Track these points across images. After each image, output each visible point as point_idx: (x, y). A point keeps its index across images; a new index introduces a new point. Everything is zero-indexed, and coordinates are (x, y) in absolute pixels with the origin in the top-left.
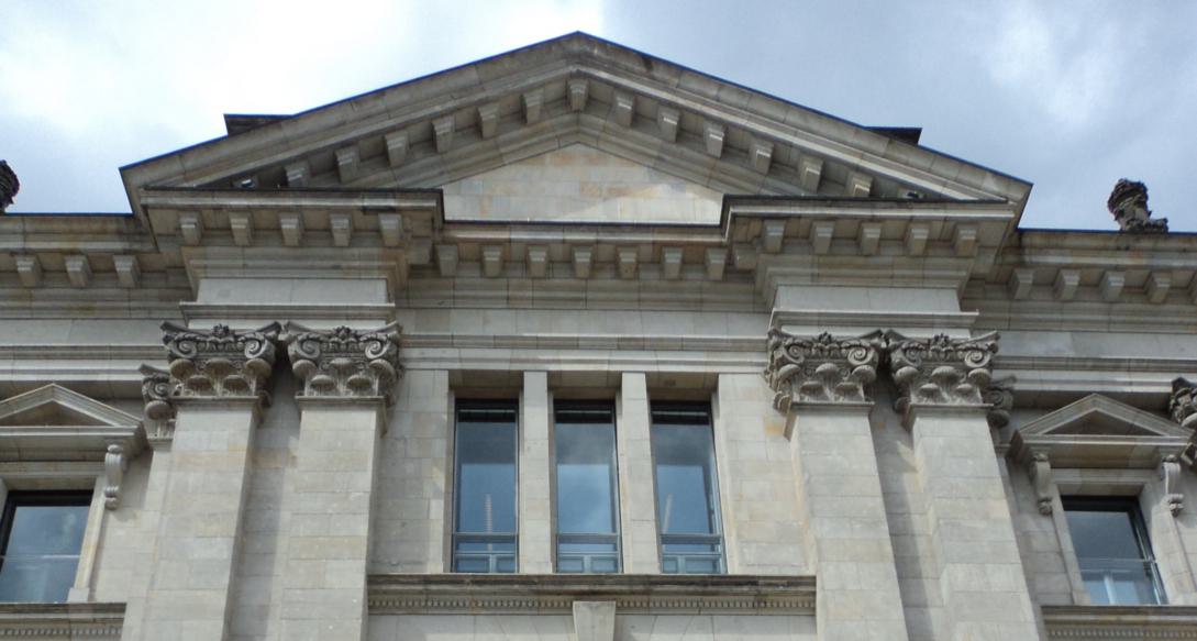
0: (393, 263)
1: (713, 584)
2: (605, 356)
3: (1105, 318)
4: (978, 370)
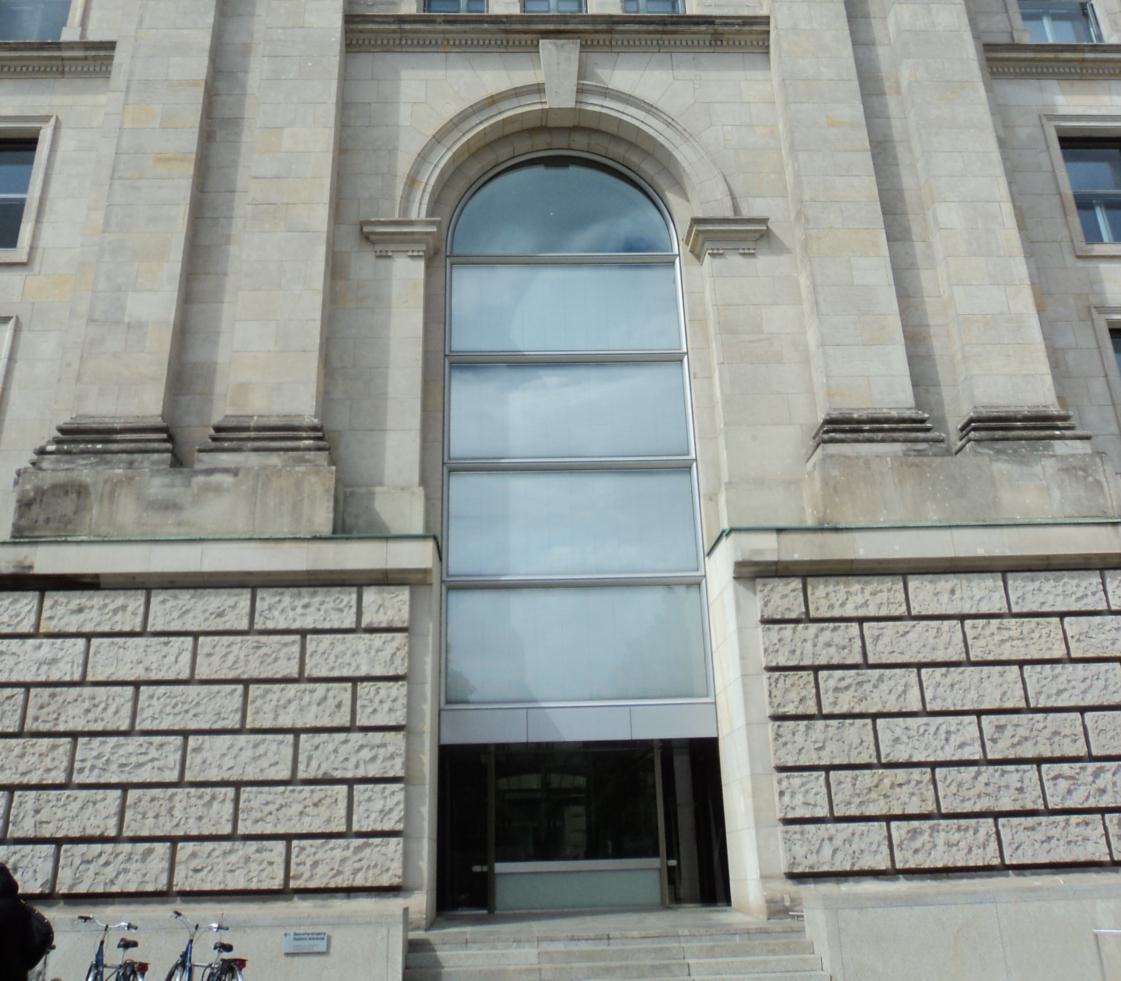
1: (673, 23)
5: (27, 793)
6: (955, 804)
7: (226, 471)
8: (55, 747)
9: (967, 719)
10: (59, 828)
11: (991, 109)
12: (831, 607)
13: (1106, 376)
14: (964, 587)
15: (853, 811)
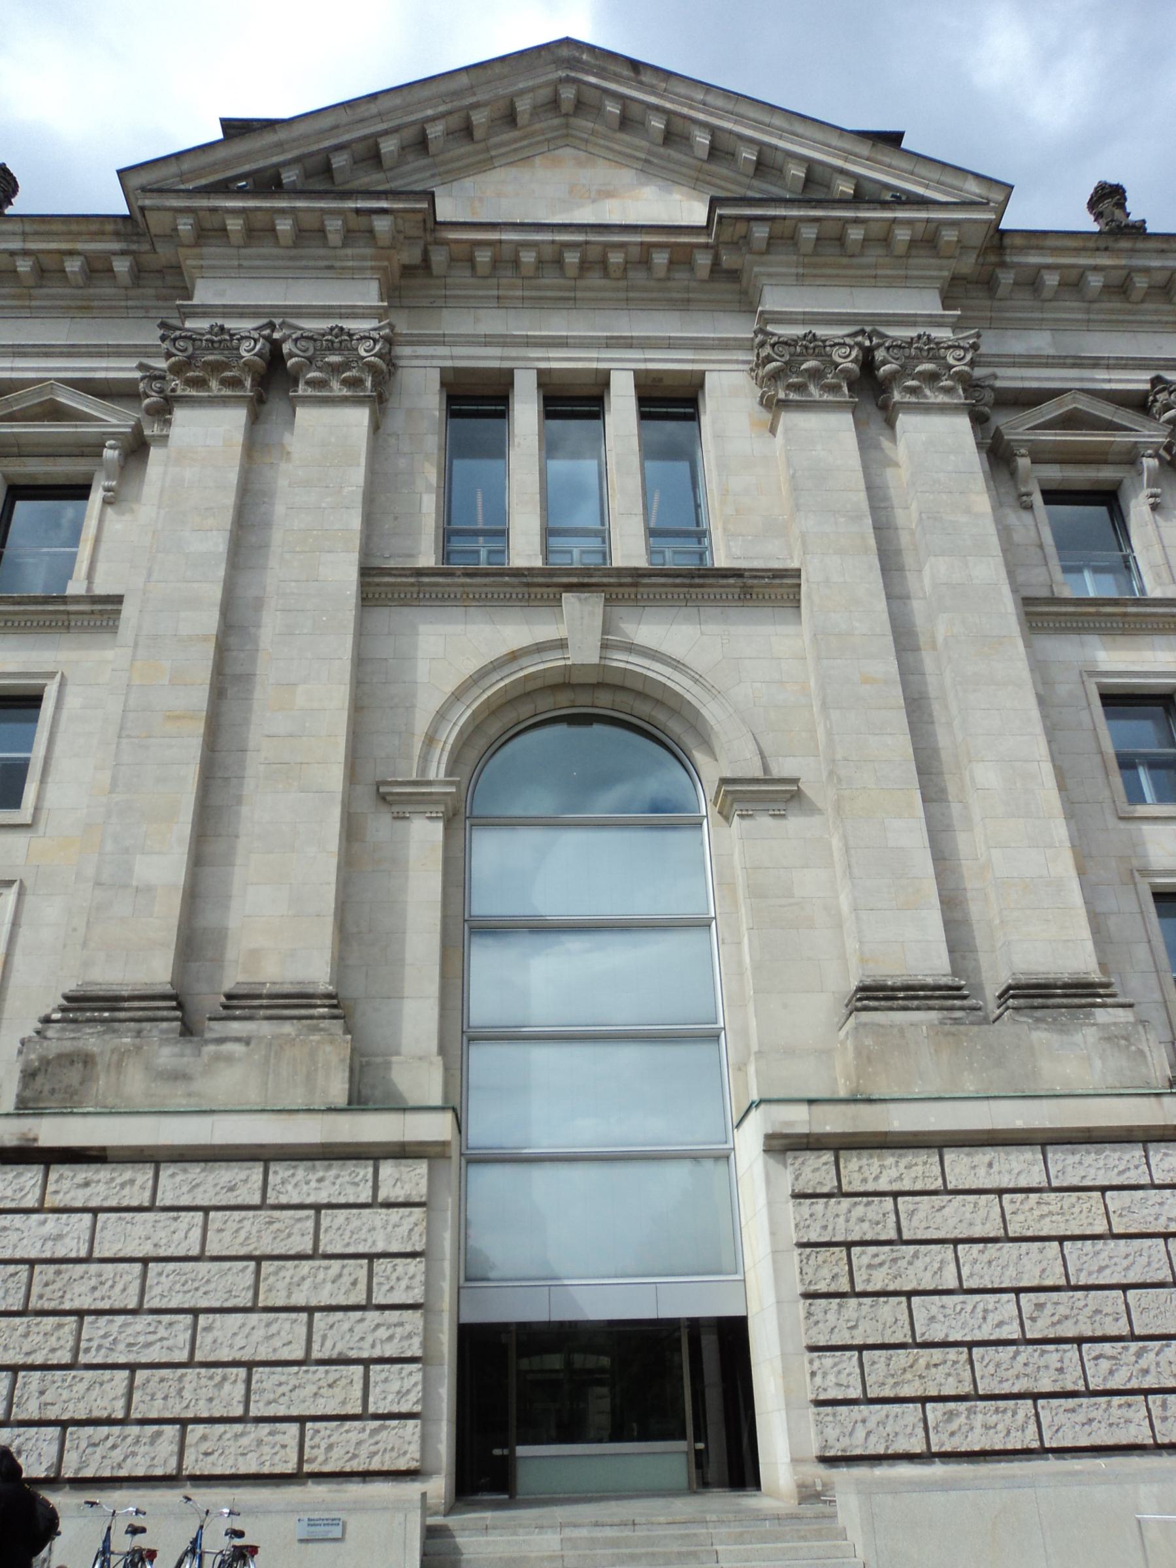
0: (386, 263)
1: (700, 576)
2: (594, 354)
3: (1085, 316)
4: (960, 367)
5: (32, 1373)
6: (992, 1386)
7: (238, 1040)
8: (60, 1326)
9: (1005, 1297)
10: (64, 1410)
11: (1030, 665)
12: (865, 1180)
13: (1149, 941)
14: (1002, 1161)
15: (887, 1392)
